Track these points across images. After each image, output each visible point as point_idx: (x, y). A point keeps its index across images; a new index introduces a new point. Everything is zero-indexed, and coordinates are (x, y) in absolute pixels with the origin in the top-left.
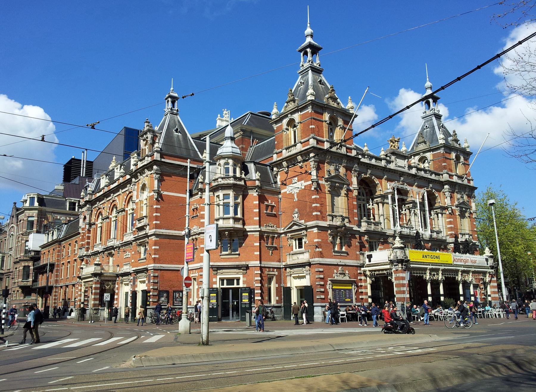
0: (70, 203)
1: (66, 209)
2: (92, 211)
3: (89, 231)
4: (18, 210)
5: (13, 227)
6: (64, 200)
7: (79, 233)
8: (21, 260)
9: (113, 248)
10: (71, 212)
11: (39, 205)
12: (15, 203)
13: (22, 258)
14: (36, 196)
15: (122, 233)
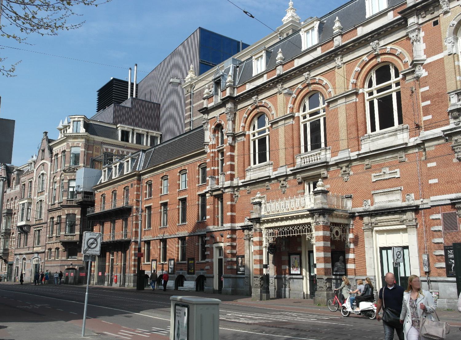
0: (123, 132)
1: (117, 139)
2: (235, 114)
3: (232, 148)
4: (50, 141)
5: (43, 164)
6: (115, 127)
7: (204, 153)
8: (63, 206)
9: (326, 165)
10: (124, 143)
11: (86, 131)
12: (46, 133)
13: (65, 203)
14: (82, 119)
15: (354, 135)
